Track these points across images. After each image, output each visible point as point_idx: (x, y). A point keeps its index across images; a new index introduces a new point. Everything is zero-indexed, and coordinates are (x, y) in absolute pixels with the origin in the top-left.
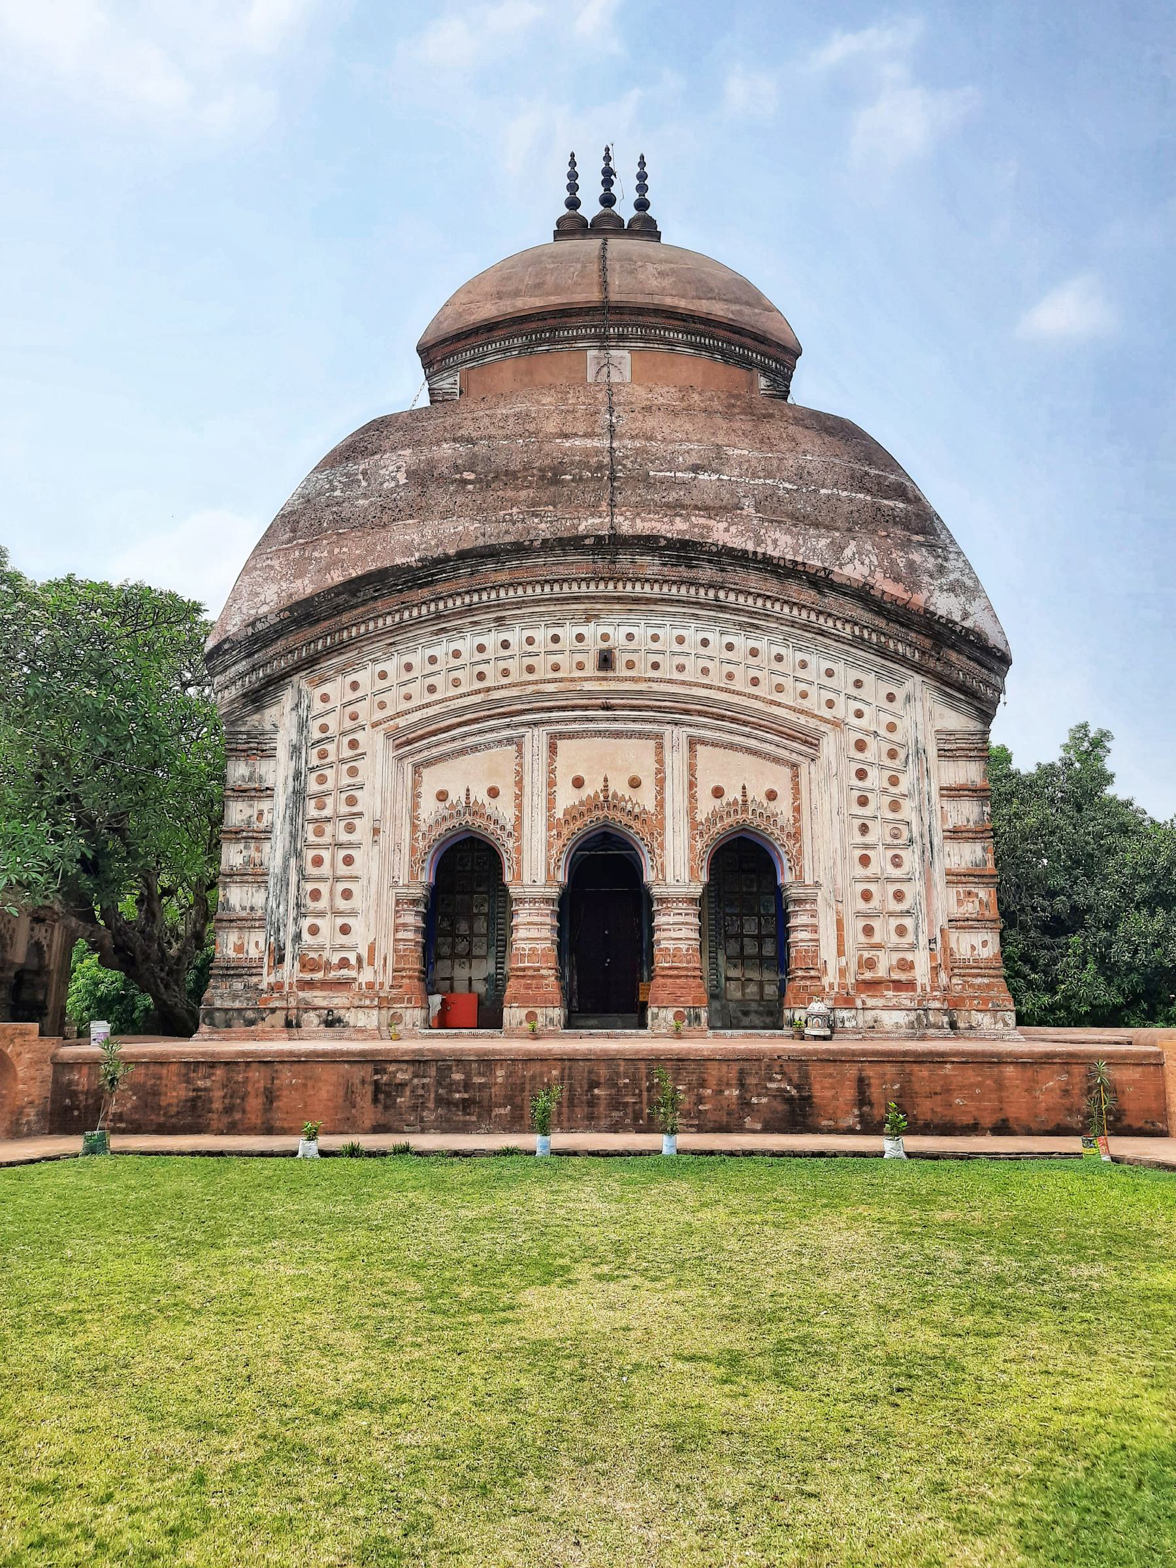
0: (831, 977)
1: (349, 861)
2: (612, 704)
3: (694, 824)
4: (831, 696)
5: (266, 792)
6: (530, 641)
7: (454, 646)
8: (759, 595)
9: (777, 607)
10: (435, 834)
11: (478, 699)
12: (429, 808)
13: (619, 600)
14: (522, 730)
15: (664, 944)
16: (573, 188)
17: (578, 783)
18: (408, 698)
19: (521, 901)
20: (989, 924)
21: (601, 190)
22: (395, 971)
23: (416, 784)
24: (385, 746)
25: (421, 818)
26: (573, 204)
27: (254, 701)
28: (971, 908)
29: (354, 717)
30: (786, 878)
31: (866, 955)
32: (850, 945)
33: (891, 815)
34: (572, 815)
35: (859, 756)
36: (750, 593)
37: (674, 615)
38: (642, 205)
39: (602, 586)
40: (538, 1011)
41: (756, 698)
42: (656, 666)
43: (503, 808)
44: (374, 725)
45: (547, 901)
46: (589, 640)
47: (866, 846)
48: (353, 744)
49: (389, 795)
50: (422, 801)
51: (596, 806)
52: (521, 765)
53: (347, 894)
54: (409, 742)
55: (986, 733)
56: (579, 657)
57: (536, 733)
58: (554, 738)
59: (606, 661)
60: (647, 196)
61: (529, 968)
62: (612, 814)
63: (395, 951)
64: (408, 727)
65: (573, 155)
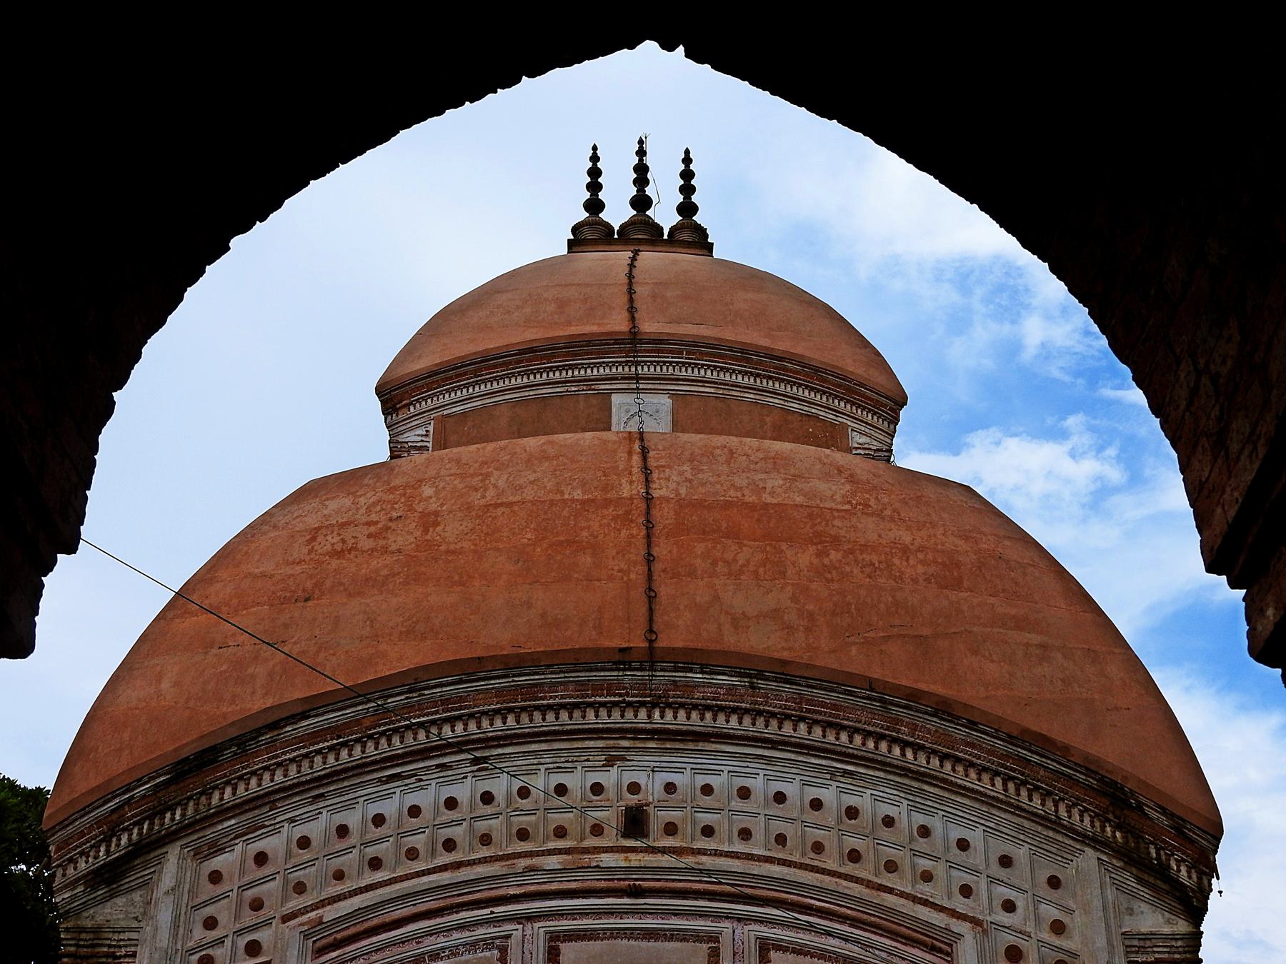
4: (967, 879)
6: (524, 793)
7: (412, 799)
8: (857, 730)
9: (883, 746)
11: (446, 877)
14: (508, 927)
16: (594, 187)
18: (339, 876)
21: (633, 191)
24: (302, 954)
26: (594, 206)
27: (109, 883)
36: (844, 728)
37: (732, 755)
38: (688, 209)
39: (629, 714)
41: (857, 880)
42: (708, 831)
44: (286, 919)
46: (611, 792)
55: (1195, 939)
57: (528, 932)
58: (555, 938)
59: (635, 822)
60: (694, 198)
65: (595, 148)
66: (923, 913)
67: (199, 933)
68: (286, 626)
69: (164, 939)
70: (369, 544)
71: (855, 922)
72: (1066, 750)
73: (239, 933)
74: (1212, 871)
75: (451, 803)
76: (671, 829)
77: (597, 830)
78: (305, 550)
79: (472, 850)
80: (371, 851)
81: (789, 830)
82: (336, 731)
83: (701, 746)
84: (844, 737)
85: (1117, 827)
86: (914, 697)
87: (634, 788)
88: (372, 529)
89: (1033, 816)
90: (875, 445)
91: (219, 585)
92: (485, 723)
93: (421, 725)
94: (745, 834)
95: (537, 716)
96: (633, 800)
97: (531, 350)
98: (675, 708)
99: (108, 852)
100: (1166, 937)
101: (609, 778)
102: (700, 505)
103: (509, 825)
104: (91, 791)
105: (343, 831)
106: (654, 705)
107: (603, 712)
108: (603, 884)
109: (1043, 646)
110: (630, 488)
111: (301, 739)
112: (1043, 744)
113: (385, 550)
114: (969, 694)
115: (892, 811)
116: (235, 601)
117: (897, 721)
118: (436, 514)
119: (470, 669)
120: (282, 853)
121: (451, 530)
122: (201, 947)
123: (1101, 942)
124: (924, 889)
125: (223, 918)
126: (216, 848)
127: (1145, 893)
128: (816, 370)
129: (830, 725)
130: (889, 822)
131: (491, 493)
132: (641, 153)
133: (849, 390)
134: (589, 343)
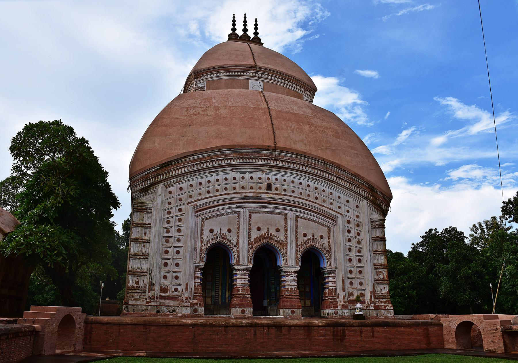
0: (341, 298)
1: (178, 252)
3: (297, 246)
4: (340, 205)
5: (149, 226)
6: (243, 178)
7: (217, 177)
8: (319, 170)
9: (325, 174)
10: (209, 245)
11: (226, 197)
14: (240, 209)
15: (287, 287)
16: (234, 25)
17: (259, 229)
19: (239, 270)
20: (386, 282)
23: (202, 226)
24: (192, 213)
25: (204, 238)
26: (234, 29)
28: (381, 276)
31: (350, 291)
32: (346, 288)
33: (358, 245)
34: (256, 240)
35: (348, 225)
38: (256, 33)
40: (245, 309)
41: (317, 204)
42: (285, 190)
44: (188, 204)
45: (248, 270)
47: (350, 256)
48: (180, 210)
49: (193, 230)
50: (204, 232)
52: (239, 221)
55: (384, 220)
56: (260, 185)
58: (250, 212)
59: (269, 187)
60: (258, 31)
61: (241, 294)
64: (200, 205)
67: (167, 205)
68: (186, 132)
69: (159, 206)
70: (202, 113)
71: (316, 213)
72: (363, 178)
73: (177, 206)
74: (389, 206)
75: (226, 179)
76: (277, 189)
77: (260, 188)
78: (186, 113)
79: (231, 190)
80: (208, 189)
83: (284, 170)
84: (316, 171)
85: (372, 196)
86: (332, 163)
87: (268, 179)
89: (355, 192)
90: (309, 100)
91: (165, 120)
93: (220, 160)
94: (293, 191)
95: (247, 160)
96: (268, 182)
97: (231, 66)
98: (279, 161)
100: (379, 220)
101: (264, 176)
102: (280, 112)
103: (240, 186)
104: (141, 169)
105: (200, 184)
106: (275, 160)
107: (263, 161)
108: (261, 201)
109: (357, 154)
110: (264, 106)
111: (192, 161)
112: (358, 176)
113: (207, 115)
114: (344, 163)
115: (325, 189)
116: (171, 124)
117: (328, 168)
118: (218, 107)
119: (233, 147)
120: (186, 188)
121: (223, 111)
122: (168, 209)
123: (367, 220)
124: (331, 207)
126: (170, 186)
127: (375, 210)
128: (297, 80)
129: (313, 168)
130: (324, 191)
131: (230, 103)
132: (245, 18)
133: (304, 86)
134: (245, 66)
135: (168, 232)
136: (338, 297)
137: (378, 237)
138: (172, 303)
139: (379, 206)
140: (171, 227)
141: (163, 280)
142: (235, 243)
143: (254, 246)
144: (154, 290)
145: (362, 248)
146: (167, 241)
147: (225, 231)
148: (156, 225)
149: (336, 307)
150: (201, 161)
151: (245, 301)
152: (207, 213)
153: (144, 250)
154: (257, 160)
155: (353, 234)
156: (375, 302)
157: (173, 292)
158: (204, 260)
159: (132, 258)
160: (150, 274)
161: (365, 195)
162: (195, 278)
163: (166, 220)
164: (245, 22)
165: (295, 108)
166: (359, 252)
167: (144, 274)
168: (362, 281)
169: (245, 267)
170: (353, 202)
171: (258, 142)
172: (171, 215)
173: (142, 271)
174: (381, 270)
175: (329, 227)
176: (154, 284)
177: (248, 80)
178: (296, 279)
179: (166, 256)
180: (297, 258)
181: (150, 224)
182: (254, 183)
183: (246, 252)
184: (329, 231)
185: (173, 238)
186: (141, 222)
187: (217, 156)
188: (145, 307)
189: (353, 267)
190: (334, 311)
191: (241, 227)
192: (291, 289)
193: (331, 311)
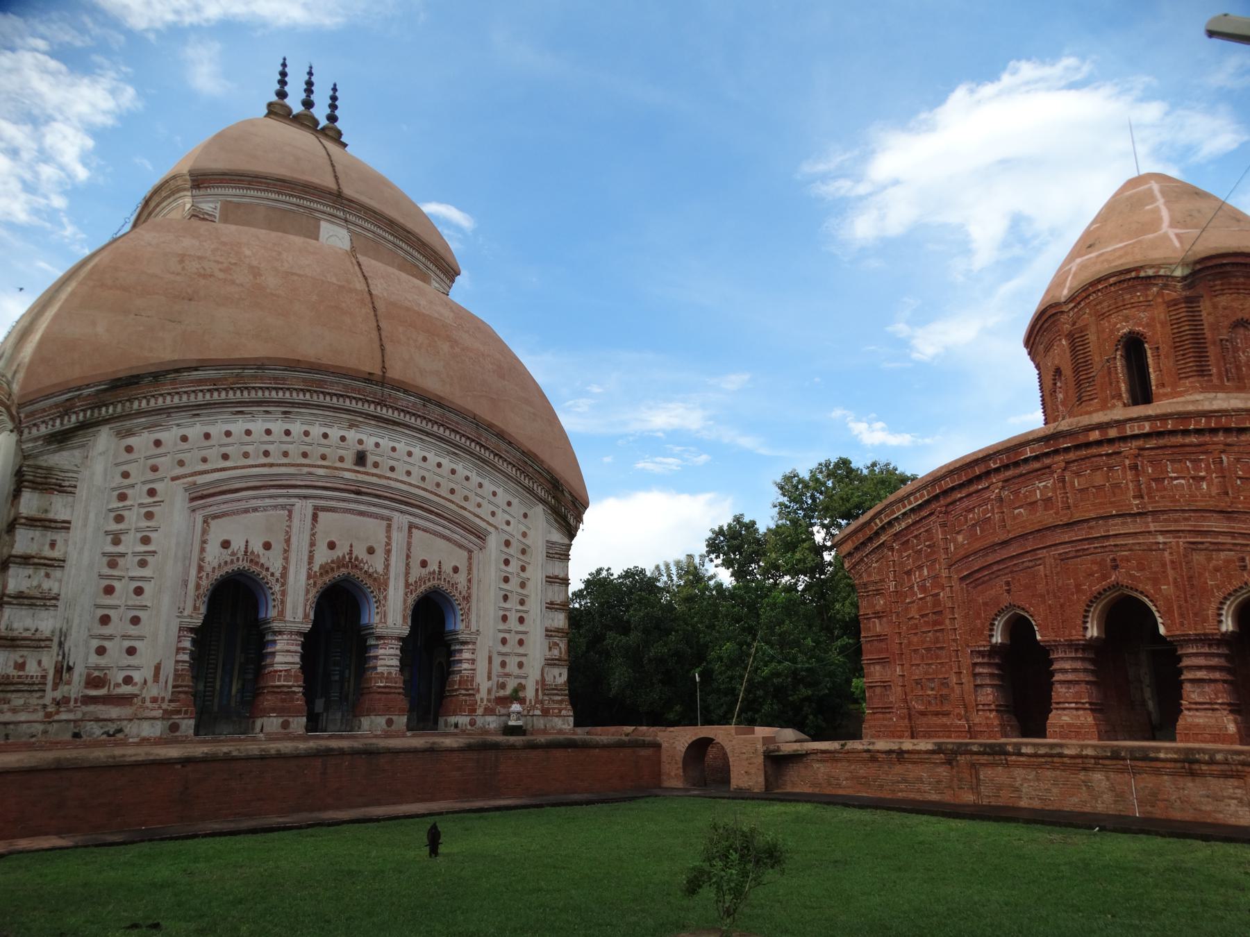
0: (483, 694)
1: (139, 591)
2: (362, 490)
3: (407, 585)
4: (494, 509)
5: (65, 526)
6: (306, 434)
7: (250, 426)
10: (217, 575)
12: (214, 555)
13: (375, 418)
15: (380, 669)
16: (283, 82)
17: (332, 546)
18: (204, 460)
19: (280, 633)
21: (304, 96)
22: (174, 687)
25: (207, 560)
26: (282, 94)
27: (60, 442)
28: (556, 652)
29: (154, 469)
30: (458, 625)
31: (501, 680)
33: (520, 591)
34: (325, 569)
35: (506, 550)
38: (332, 118)
39: (366, 405)
40: (291, 719)
41: (453, 502)
43: (273, 561)
44: (173, 479)
47: (506, 609)
48: (152, 493)
50: (208, 547)
51: (343, 566)
52: (289, 527)
53: (135, 621)
54: (202, 497)
56: (342, 452)
58: (316, 508)
59: (361, 458)
62: (353, 572)
63: (176, 670)
64: (204, 485)
66: (477, 521)
67: (118, 480)
69: (98, 479)
70: (221, 275)
73: (144, 483)
75: (268, 432)
76: (376, 465)
81: (426, 474)
82: (214, 381)
86: (490, 427)
87: (360, 442)
88: (220, 266)
92: (294, 394)
93: (261, 388)
94: (409, 473)
95: (321, 396)
96: (360, 448)
99: (62, 424)
101: (352, 435)
104: (54, 386)
105: (207, 436)
110: (360, 285)
111: (192, 382)
113: (233, 282)
115: (469, 474)
119: (293, 365)
121: (271, 281)
122: (120, 488)
124: (477, 511)
125: (132, 475)
126: (130, 433)
127: (557, 525)
130: (467, 478)
135: (116, 542)
136: (478, 690)
137: (557, 577)
138: (114, 712)
139: (565, 518)
140: (126, 532)
141: (94, 659)
142: (278, 575)
143: (320, 582)
144: (69, 683)
145: (526, 596)
146: (112, 565)
147: (257, 547)
148: (85, 526)
149: (473, 711)
150: (215, 386)
151: (292, 700)
152: (218, 505)
153: (46, 586)
154: (341, 400)
155: (514, 567)
156: (542, 702)
157: (118, 685)
158: (203, 609)
159: (9, 603)
160: (61, 644)
161: (542, 494)
162: (178, 650)
163: (113, 515)
164: (310, 84)
165: (423, 302)
166: (522, 603)
167: (43, 644)
168: (523, 659)
169: (295, 628)
170: (518, 508)
171: (350, 361)
172: (127, 503)
173: (38, 636)
174: (556, 640)
175: (470, 552)
176: (70, 669)
177: (319, 220)
178: (398, 652)
179: (108, 601)
180: (405, 610)
181: (69, 522)
182: (329, 446)
183: (302, 593)
184: (470, 558)
185: (129, 557)
186: (43, 516)
187: (255, 377)
188: (40, 727)
189: (509, 631)
190: (468, 719)
191: (294, 540)
192: (390, 673)
193: (463, 720)
